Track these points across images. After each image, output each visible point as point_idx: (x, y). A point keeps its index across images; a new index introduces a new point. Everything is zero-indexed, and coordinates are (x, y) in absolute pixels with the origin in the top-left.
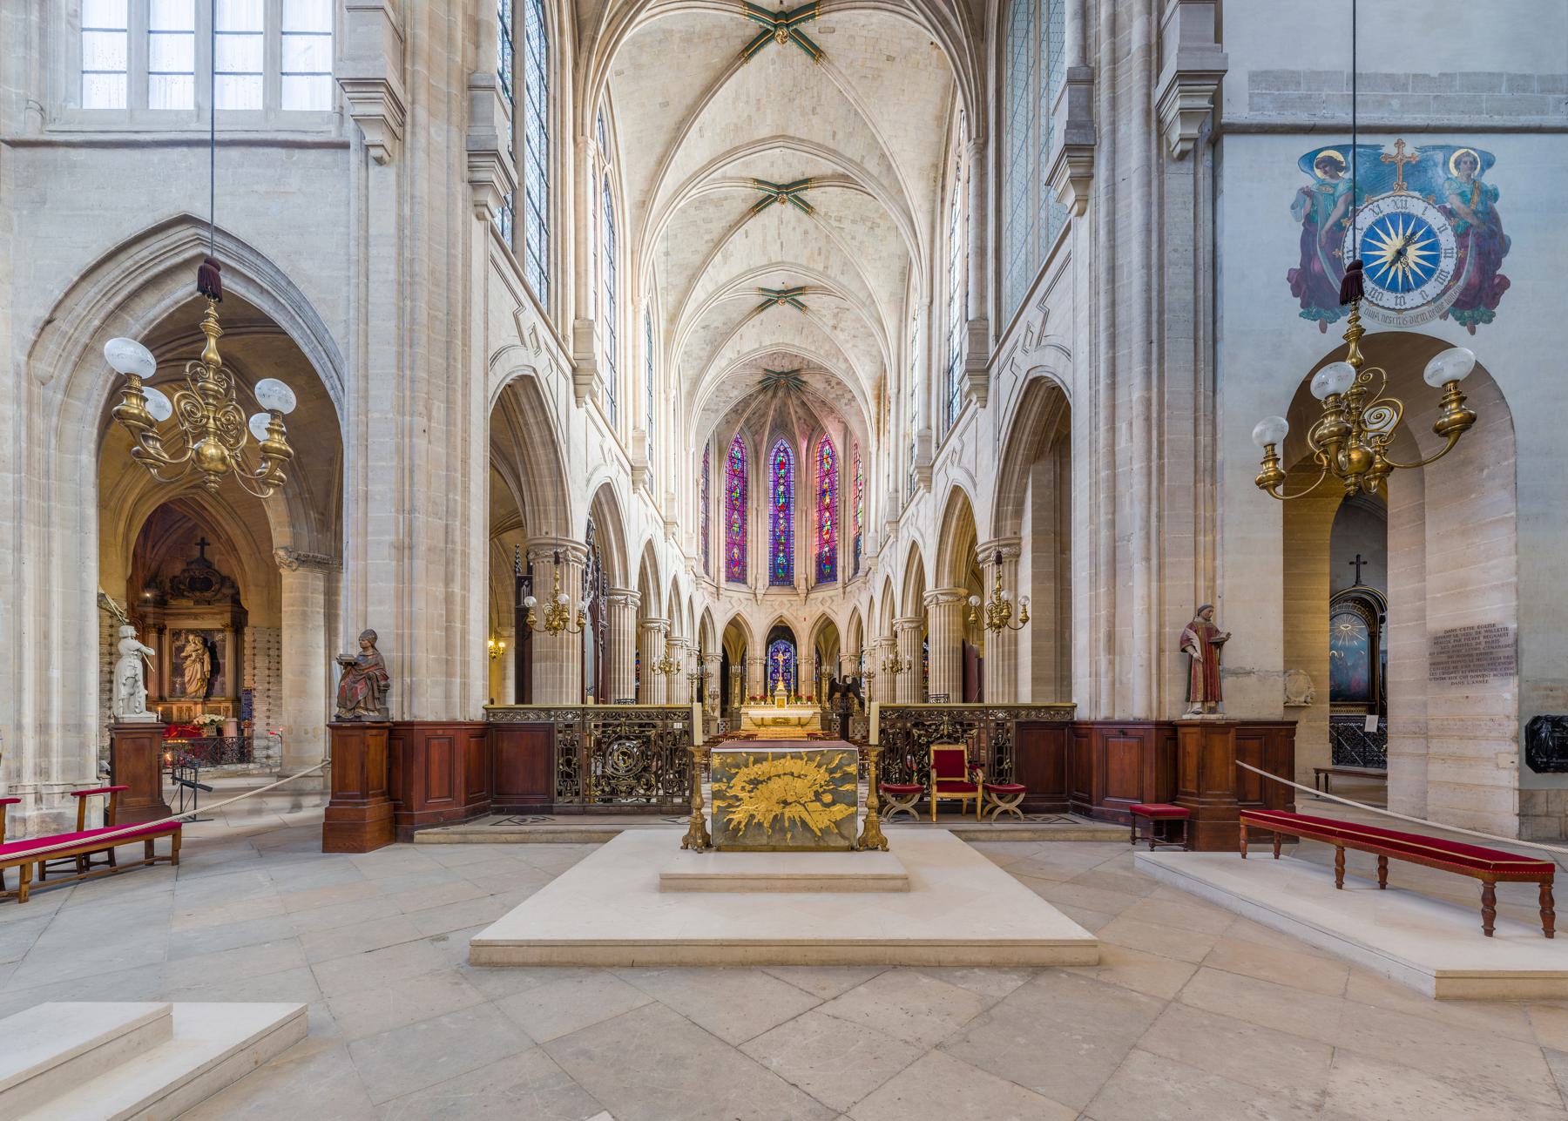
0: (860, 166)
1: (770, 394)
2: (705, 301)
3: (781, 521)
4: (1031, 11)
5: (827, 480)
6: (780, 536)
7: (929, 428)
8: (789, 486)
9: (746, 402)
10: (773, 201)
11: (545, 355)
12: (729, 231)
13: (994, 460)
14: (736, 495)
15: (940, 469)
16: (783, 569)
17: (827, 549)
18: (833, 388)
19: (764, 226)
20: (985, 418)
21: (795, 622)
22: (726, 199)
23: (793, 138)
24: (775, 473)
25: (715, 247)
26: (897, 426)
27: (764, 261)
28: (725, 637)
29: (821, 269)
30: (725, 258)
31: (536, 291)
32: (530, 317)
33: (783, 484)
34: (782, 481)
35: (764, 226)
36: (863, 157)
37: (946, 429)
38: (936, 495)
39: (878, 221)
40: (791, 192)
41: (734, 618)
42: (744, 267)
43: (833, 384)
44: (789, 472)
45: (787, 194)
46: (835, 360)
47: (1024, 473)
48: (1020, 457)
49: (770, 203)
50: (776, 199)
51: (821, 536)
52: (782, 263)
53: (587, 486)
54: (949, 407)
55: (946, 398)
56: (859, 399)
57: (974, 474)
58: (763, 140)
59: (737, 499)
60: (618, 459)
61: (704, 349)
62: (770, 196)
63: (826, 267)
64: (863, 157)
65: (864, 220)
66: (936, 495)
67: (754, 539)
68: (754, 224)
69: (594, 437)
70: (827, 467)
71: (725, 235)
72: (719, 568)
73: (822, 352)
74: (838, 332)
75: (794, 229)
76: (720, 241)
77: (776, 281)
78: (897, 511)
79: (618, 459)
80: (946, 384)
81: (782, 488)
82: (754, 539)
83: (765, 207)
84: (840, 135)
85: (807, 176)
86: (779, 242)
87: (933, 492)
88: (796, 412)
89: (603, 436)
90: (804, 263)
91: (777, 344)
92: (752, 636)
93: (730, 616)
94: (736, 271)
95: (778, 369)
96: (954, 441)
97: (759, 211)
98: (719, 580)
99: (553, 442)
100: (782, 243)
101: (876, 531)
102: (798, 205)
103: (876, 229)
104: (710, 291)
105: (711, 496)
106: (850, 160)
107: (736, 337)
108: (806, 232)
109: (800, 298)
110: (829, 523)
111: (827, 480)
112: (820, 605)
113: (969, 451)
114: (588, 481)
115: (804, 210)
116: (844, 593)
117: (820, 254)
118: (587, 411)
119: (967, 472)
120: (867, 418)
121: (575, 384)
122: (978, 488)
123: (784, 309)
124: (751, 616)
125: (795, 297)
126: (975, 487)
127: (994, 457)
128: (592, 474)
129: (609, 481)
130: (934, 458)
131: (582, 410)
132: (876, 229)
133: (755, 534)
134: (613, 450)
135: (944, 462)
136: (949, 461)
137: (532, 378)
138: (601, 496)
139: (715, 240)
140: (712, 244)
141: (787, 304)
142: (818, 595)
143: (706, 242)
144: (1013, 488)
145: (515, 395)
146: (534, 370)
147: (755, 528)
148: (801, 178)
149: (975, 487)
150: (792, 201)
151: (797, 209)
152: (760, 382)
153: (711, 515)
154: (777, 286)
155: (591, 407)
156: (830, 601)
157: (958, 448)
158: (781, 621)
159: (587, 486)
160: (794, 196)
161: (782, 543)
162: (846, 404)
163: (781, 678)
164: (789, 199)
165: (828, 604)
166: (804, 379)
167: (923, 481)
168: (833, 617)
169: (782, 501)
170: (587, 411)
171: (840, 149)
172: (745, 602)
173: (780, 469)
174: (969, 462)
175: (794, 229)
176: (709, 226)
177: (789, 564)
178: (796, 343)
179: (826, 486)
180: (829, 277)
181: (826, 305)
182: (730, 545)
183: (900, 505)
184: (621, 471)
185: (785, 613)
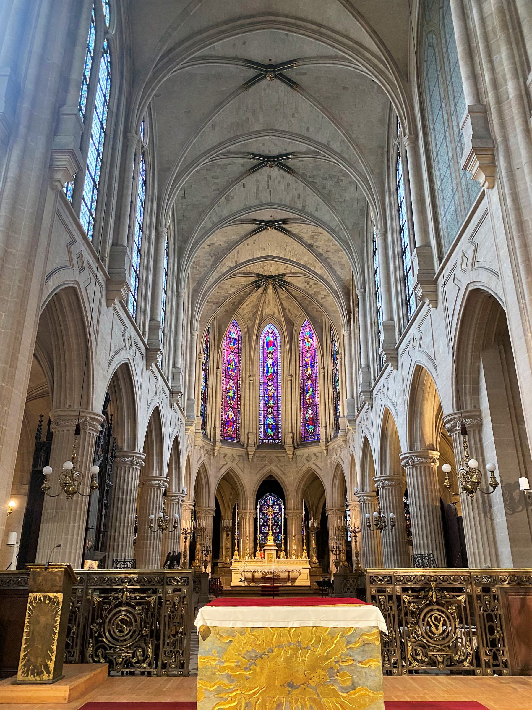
0: (327, 147)
1: (261, 290)
3: (270, 388)
4: (439, 68)
5: (308, 355)
6: (269, 401)
7: (392, 319)
8: (277, 360)
10: (264, 166)
11: (87, 272)
12: (231, 184)
13: (449, 349)
14: (232, 367)
15: (404, 351)
16: (271, 429)
17: (310, 412)
18: (311, 286)
19: (257, 181)
20: (437, 315)
21: (283, 477)
22: (229, 164)
23: (279, 131)
24: (264, 349)
25: (220, 194)
26: (365, 316)
27: (257, 202)
29: (300, 206)
30: (228, 201)
31: (85, 229)
32: (81, 246)
33: (272, 358)
34: (270, 356)
35: (257, 181)
36: (329, 142)
37: (406, 321)
38: (402, 372)
39: (343, 178)
40: (277, 161)
41: (228, 474)
42: (242, 206)
43: (311, 284)
45: (274, 161)
47: (475, 360)
48: (470, 346)
49: (262, 167)
50: (266, 165)
51: (304, 400)
52: (271, 204)
53: (109, 366)
54: (407, 305)
55: (404, 298)
57: (433, 358)
59: (233, 370)
60: (136, 345)
61: (209, 260)
62: (262, 163)
63: (304, 207)
64: (329, 142)
65: (331, 177)
66: (402, 372)
67: (247, 403)
68: (251, 180)
69: (118, 329)
70: (308, 345)
71: (227, 187)
72: (215, 428)
75: (279, 182)
76: (224, 190)
77: (266, 215)
78: (370, 382)
79: (136, 345)
80: (403, 288)
81: (270, 362)
82: (247, 403)
83: (258, 169)
84: (312, 129)
85: (289, 151)
86: (268, 190)
87: (400, 369)
88: (282, 304)
89: (125, 327)
90: (288, 204)
92: (243, 491)
93: (223, 471)
94: (235, 209)
95: (267, 274)
96: (413, 331)
97: (253, 172)
98: (214, 439)
99: (85, 334)
100: (270, 191)
102: (282, 168)
103: (341, 183)
104: (215, 222)
105: (211, 368)
107: (235, 252)
108: (288, 184)
109: (285, 226)
110: (311, 390)
111: (308, 355)
112: (305, 461)
113: (427, 340)
114: (110, 363)
115: (286, 171)
117: (299, 198)
118: (115, 309)
119: (427, 355)
121: (108, 291)
122: (437, 368)
123: (272, 233)
124: (243, 471)
125: (282, 226)
126: (435, 368)
127: (448, 346)
128: (113, 357)
129: (127, 361)
130: (398, 342)
131: (111, 309)
132: (341, 183)
133: (247, 398)
134: (133, 337)
135: (407, 346)
136: (410, 346)
137: (74, 288)
138: (120, 375)
139: (221, 189)
140: (218, 192)
141: (274, 230)
142: (303, 452)
143: (214, 190)
144: (468, 370)
145: (59, 300)
146: (78, 283)
147: (247, 394)
148: (285, 152)
149: (435, 368)
150: (278, 166)
151: (282, 171)
153: (210, 383)
154: (267, 218)
155: (119, 307)
156: (314, 458)
157: (418, 336)
158: (271, 476)
159: (109, 366)
160: (279, 163)
161: (270, 407)
162: (322, 299)
163: (270, 533)
164: (276, 165)
165: (312, 461)
166: (288, 279)
167: (391, 360)
169: (271, 371)
170: (115, 309)
171: (312, 136)
172: (237, 459)
174: (428, 348)
175: (279, 182)
176: (216, 181)
177: (277, 425)
179: (308, 360)
180: (306, 213)
181: (304, 230)
182: (225, 408)
183: (372, 378)
184: (138, 352)
185: (274, 468)
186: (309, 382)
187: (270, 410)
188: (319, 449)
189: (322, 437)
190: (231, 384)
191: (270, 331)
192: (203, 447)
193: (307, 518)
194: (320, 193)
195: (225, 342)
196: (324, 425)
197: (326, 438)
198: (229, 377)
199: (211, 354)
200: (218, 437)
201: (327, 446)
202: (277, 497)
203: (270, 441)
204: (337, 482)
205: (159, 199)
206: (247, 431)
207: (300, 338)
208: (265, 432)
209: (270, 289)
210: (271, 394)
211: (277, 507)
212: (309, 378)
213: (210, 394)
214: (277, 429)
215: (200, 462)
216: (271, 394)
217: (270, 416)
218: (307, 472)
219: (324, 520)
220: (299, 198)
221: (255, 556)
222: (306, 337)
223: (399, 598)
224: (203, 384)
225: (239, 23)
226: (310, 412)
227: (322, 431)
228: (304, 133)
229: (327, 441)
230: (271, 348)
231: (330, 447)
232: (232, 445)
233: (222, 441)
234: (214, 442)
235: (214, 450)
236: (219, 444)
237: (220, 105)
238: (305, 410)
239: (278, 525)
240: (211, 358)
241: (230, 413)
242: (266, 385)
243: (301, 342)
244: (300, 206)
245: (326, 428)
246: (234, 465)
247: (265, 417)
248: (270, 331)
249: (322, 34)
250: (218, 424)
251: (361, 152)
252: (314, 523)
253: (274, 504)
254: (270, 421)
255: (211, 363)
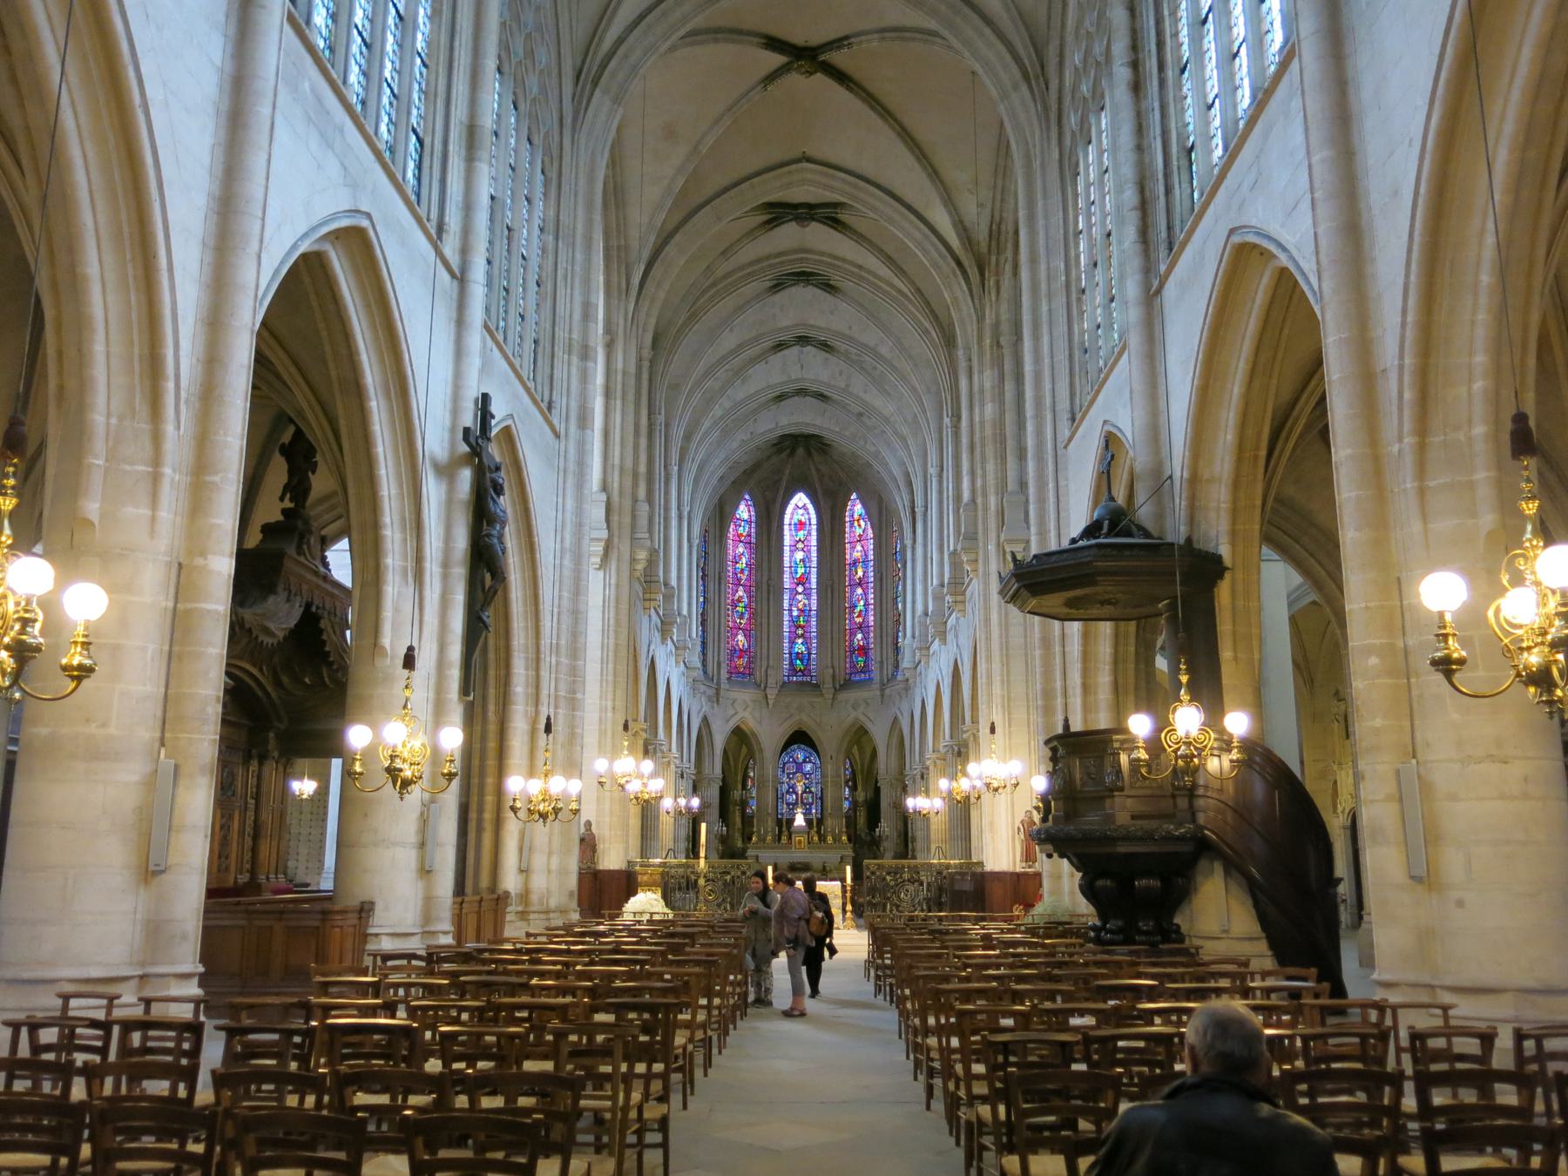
1: (784, 455)
2: (722, 417)
5: (859, 548)
8: (809, 551)
9: (756, 467)
16: (802, 661)
17: (859, 636)
23: (812, 326)
24: (791, 535)
27: (784, 378)
28: (725, 752)
29: (843, 385)
34: (800, 545)
44: (809, 534)
46: (862, 442)
56: (891, 485)
58: (787, 327)
59: (742, 571)
67: (765, 621)
70: (859, 531)
73: (847, 433)
74: (865, 419)
81: (799, 555)
88: (818, 470)
91: (797, 424)
92: (761, 751)
98: (719, 679)
101: (914, 637)
105: (710, 572)
106: (865, 346)
110: (862, 603)
111: (859, 548)
116: (882, 696)
117: (841, 374)
120: (900, 507)
124: (760, 723)
140: (731, 373)
147: (765, 608)
152: (775, 445)
153: (710, 595)
165: (861, 709)
168: (869, 726)
169: (801, 571)
173: (798, 530)
177: (809, 654)
178: (818, 422)
179: (857, 555)
185: (805, 718)
186: (859, 591)
187: (800, 632)
188: (872, 693)
189: (876, 675)
190: (741, 593)
191: (800, 505)
192: (704, 693)
193: (854, 789)
194: (870, 375)
195: (732, 526)
196: (879, 659)
197: (881, 679)
198: (738, 583)
199: (711, 550)
200: (724, 675)
201: (882, 690)
202: (810, 750)
203: (800, 679)
204: (895, 740)
205: (667, 425)
206: (764, 663)
207: (847, 519)
208: (791, 663)
209: (801, 451)
210: (800, 606)
211: (808, 767)
212: (860, 584)
213: (710, 612)
214: (809, 659)
215: (701, 714)
216: (800, 606)
217: (800, 641)
218: (853, 725)
219: (877, 790)
220: (841, 374)
221: (780, 839)
222: (856, 517)
223: (884, 879)
224: (701, 599)
225: (765, 264)
226: (859, 636)
227: (874, 666)
228: (847, 332)
229: (883, 687)
230: (801, 534)
231: (887, 692)
232: (743, 685)
233: (729, 679)
234: (719, 683)
235: (718, 694)
236: (724, 685)
237: (740, 309)
238: (853, 634)
239: (811, 792)
240: (711, 557)
241: (741, 638)
242: (794, 593)
243: (847, 525)
244: (843, 385)
245: (882, 662)
246: (747, 714)
247: (792, 643)
248: (800, 505)
249: (862, 278)
250: (724, 657)
251: (916, 365)
252: (861, 796)
253: (804, 761)
254: (800, 647)
255: (711, 564)
